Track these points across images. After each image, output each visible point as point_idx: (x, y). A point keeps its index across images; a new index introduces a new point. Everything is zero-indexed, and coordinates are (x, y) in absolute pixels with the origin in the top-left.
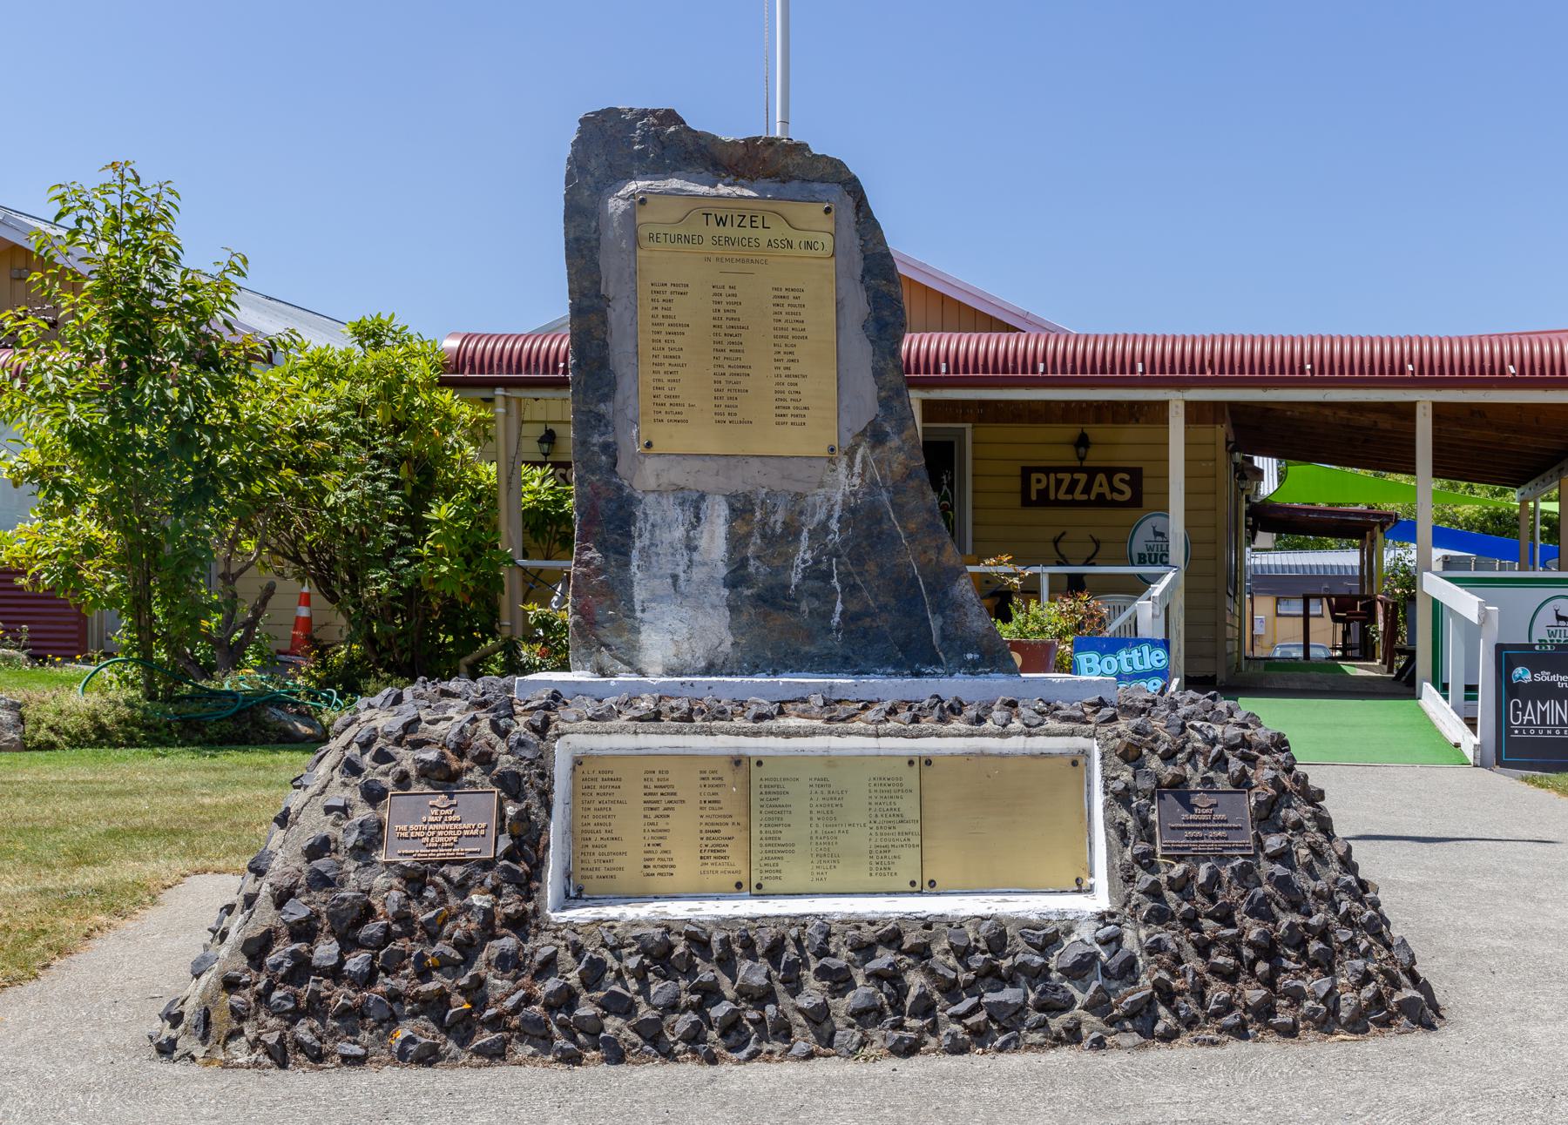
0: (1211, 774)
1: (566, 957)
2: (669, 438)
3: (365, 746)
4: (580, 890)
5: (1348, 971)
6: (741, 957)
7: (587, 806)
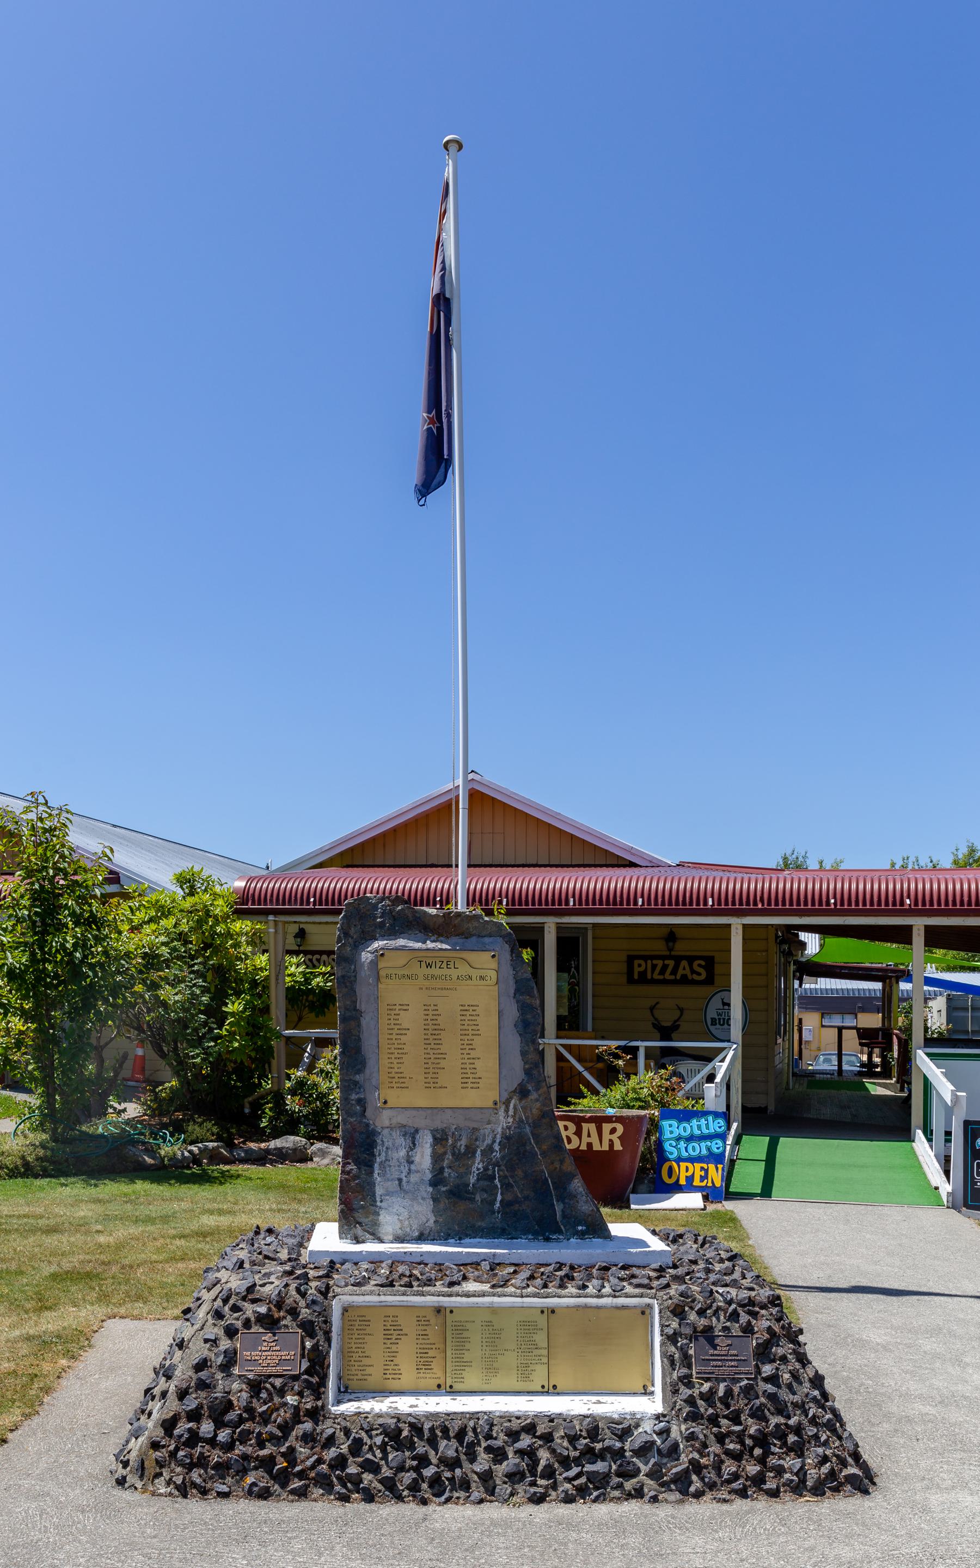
0: (728, 1324)
1: (340, 1435)
2: (396, 1098)
3: (225, 1301)
4: (347, 1388)
5: (812, 1455)
6: (441, 1438)
7: (351, 1336)
